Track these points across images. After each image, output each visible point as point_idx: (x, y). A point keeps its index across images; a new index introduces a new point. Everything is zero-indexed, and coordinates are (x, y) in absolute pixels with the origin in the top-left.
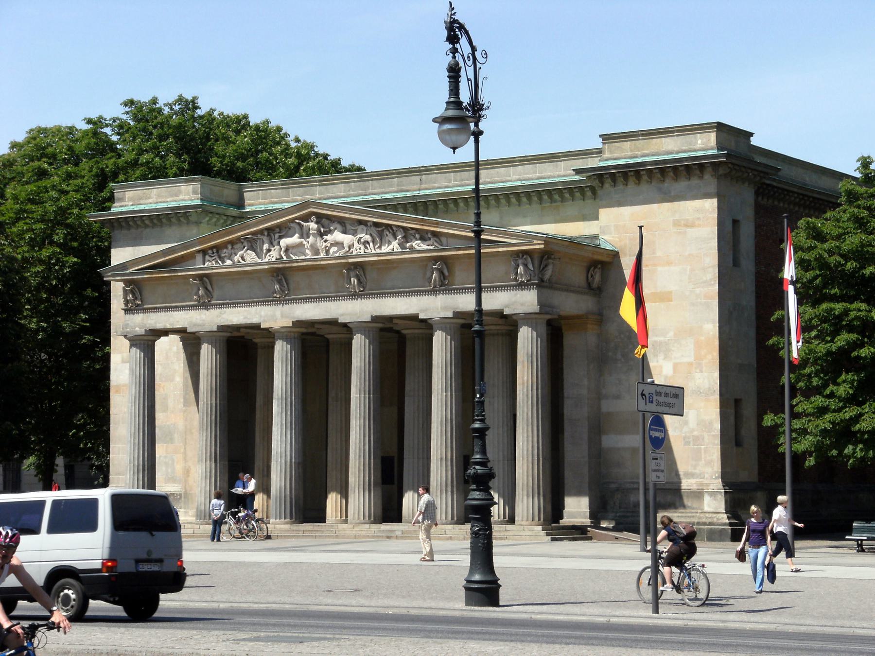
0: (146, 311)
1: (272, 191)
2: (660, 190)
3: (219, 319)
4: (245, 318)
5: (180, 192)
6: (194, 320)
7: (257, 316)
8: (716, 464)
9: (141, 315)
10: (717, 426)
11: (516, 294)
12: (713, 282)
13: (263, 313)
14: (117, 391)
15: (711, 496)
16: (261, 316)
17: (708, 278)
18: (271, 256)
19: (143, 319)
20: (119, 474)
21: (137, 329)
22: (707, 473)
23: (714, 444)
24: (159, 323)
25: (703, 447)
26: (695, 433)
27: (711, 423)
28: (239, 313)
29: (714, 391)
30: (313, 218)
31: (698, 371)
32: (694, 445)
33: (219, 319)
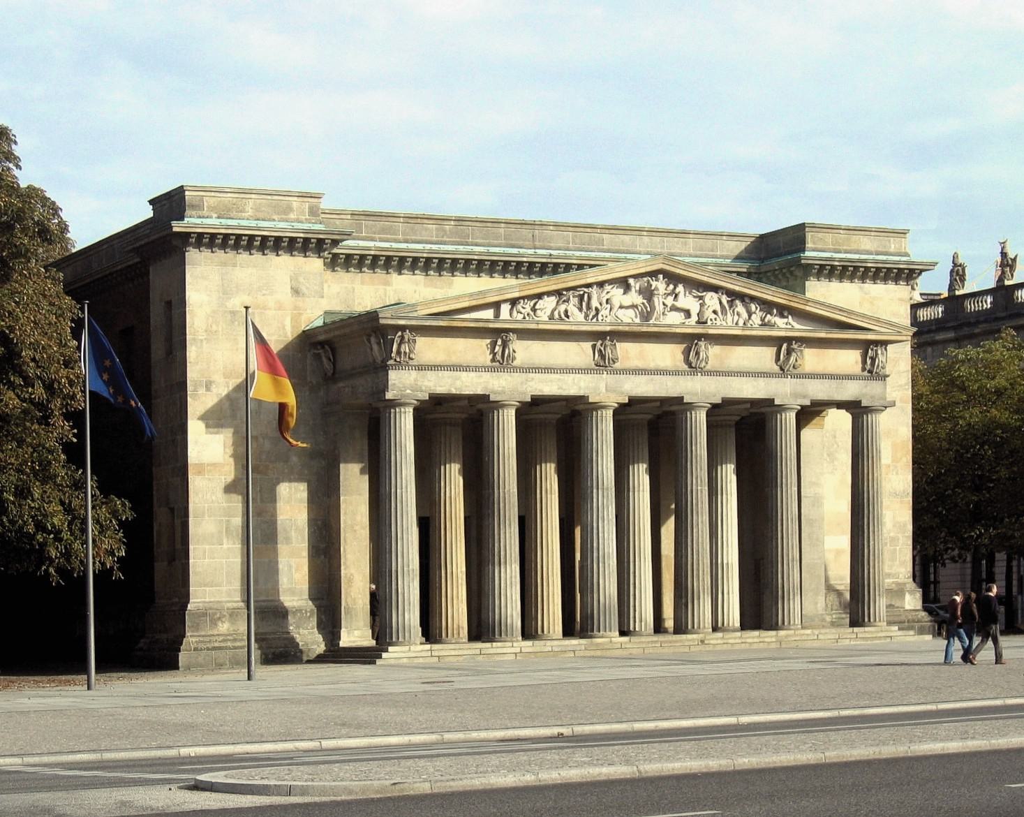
0: (421, 368)
1: (338, 222)
2: (860, 288)
3: (525, 387)
4: (559, 389)
5: (289, 209)
6: (490, 386)
7: (575, 387)
8: (908, 564)
9: (414, 374)
10: (910, 527)
11: (866, 386)
12: (907, 387)
13: (582, 384)
14: (199, 473)
15: (909, 593)
16: (580, 388)
17: (903, 383)
18: (604, 316)
19: (416, 380)
20: (205, 586)
21: (408, 391)
22: (902, 573)
23: (907, 545)
24: (441, 386)
25: (898, 548)
26: (892, 534)
27: (905, 525)
28: (551, 381)
29: (908, 494)
30: (661, 276)
31: (894, 473)
32: (890, 546)
33: (525, 387)
